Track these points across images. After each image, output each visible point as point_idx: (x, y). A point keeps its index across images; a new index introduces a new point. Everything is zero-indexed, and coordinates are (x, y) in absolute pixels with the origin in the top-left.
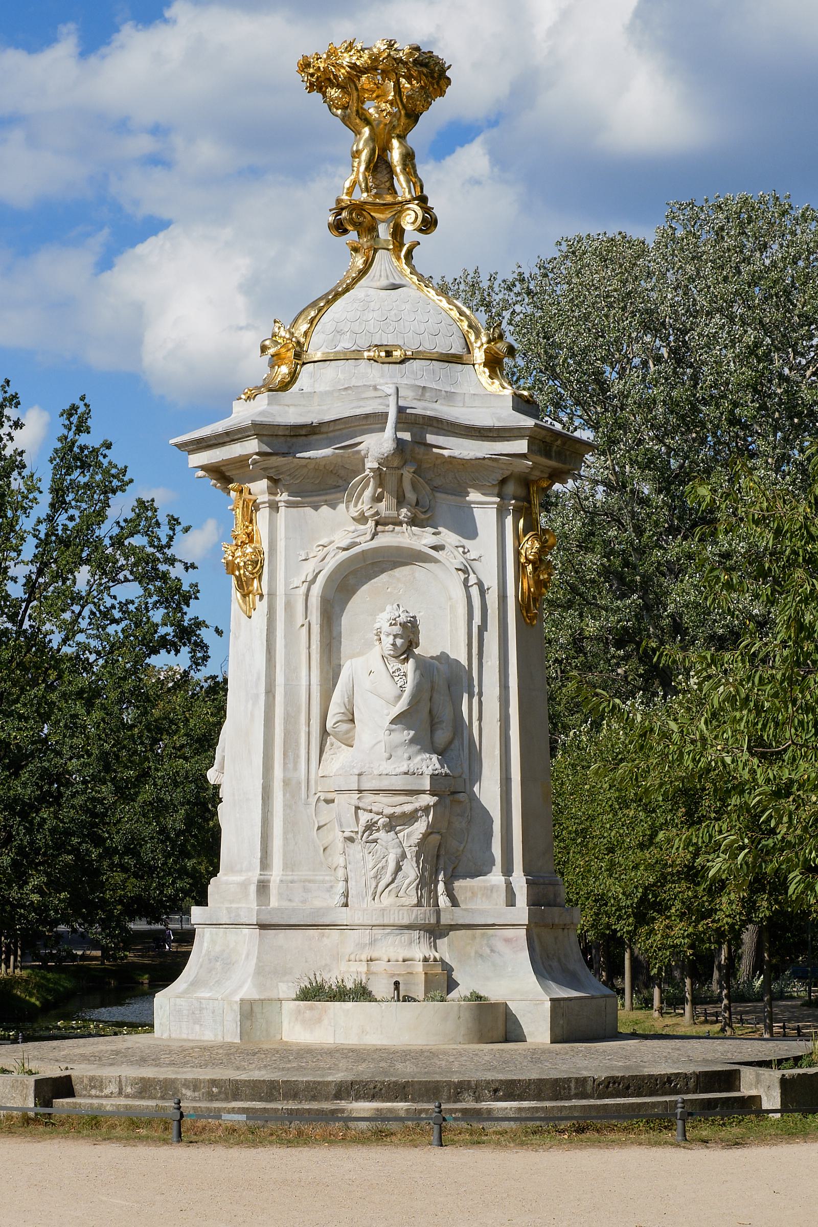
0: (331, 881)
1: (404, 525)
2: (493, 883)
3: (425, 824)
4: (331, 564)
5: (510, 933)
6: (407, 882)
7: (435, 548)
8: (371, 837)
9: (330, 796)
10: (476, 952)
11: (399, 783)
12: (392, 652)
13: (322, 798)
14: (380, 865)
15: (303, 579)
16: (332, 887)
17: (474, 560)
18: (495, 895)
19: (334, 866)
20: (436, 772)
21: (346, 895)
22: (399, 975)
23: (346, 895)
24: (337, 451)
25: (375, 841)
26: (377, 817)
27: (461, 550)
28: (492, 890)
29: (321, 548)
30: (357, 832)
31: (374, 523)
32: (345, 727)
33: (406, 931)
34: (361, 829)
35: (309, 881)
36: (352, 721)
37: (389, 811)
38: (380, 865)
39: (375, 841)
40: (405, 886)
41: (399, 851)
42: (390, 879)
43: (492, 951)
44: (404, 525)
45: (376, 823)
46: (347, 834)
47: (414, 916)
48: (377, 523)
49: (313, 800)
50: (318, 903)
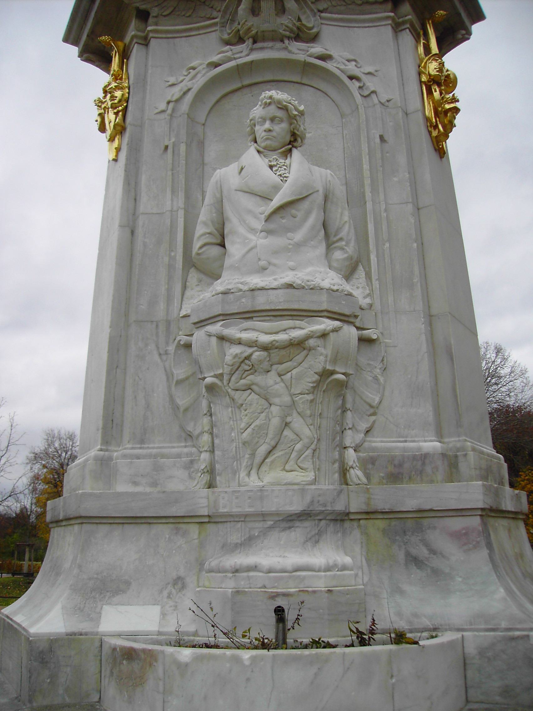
0: (191, 454)
1: (286, 41)
2: (425, 451)
3: (322, 358)
4: (200, 81)
5: (457, 524)
6: (298, 446)
8: (243, 382)
10: (408, 554)
11: (279, 300)
12: (268, 142)
13: (182, 343)
14: (257, 422)
15: (169, 98)
16: (192, 462)
17: (369, 73)
18: (428, 469)
19: (196, 433)
20: (335, 288)
21: (211, 471)
22: (285, 595)
23: (211, 471)
25: (249, 388)
26: (249, 351)
28: (424, 464)
29: (191, 71)
30: (220, 376)
31: (251, 40)
32: (216, 251)
33: (298, 524)
34: (227, 370)
35: (163, 456)
36: (223, 245)
37: (265, 339)
38: (257, 422)
39: (249, 388)
40: (294, 455)
41: (287, 399)
42: (273, 443)
43: (433, 552)
44: (286, 41)
45: (248, 358)
46: (209, 380)
47: (308, 499)
48: (255, 42)
49: (171, 348)
50: (174, 486)
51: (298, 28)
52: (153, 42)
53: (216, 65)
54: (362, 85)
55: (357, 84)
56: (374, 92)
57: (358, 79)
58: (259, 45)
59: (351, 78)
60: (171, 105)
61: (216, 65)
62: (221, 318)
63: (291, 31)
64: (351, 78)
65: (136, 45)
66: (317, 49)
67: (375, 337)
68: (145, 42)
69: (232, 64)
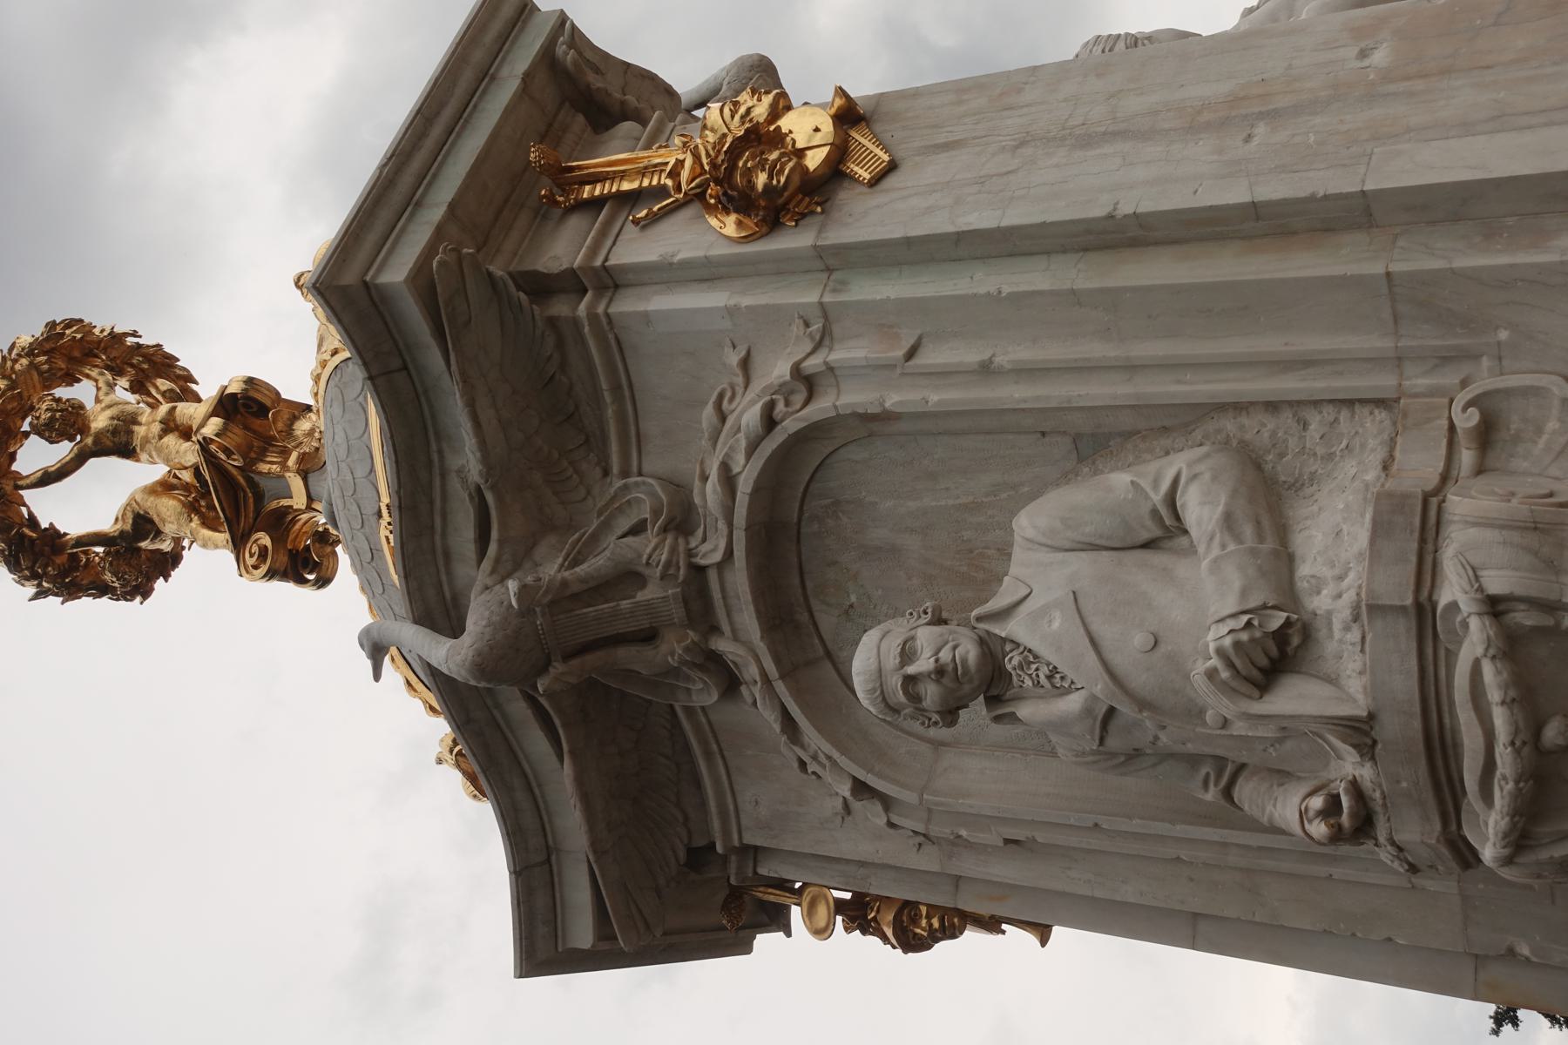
48: (715, 629)
52: (749, 839)
56: (796, 370)
57: (770, 407)
59: (770, 422)
60: (895, 819)
63: (673, 550)
66: (710, 494)
68: (754, 853)
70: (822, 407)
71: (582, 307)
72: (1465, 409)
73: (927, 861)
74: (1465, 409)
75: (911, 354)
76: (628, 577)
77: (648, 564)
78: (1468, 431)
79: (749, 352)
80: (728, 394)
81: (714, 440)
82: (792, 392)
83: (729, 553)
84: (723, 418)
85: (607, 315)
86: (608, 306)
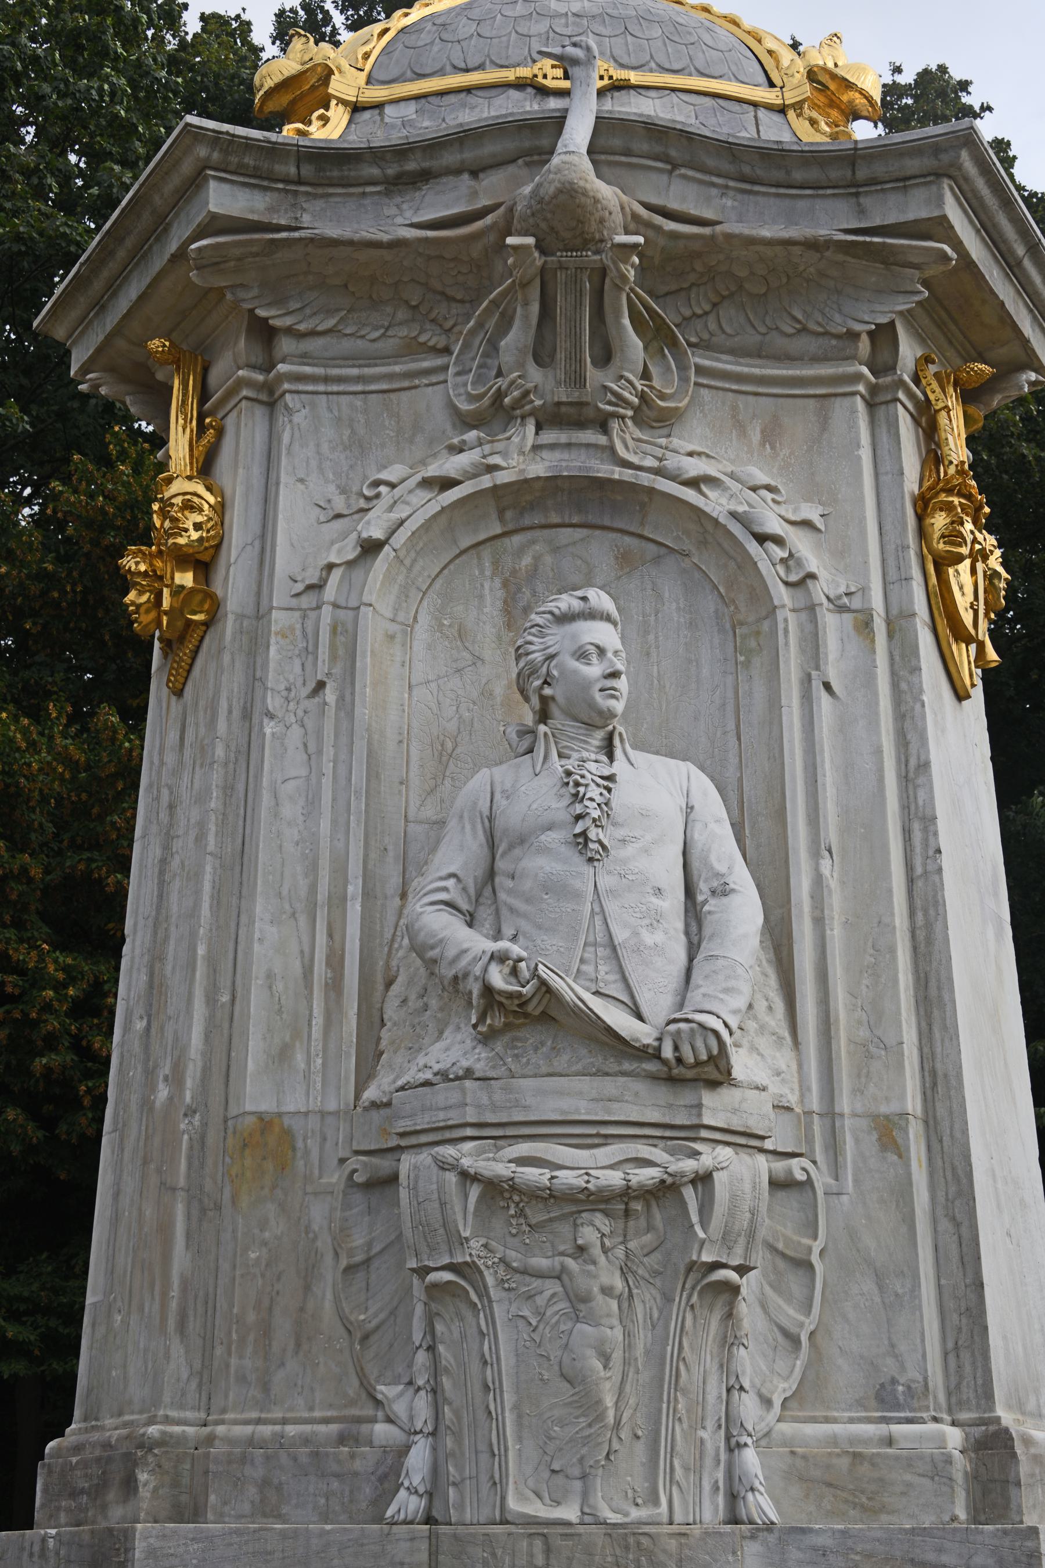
7: (694, 483)
9: (384, 1165)
24: (430, 234)
27: (769, 496)
48: (539, 428)
51: (642, 396)
53: (447, 484)
54: (786, 555)
55: (779, 553)
56: (812, 576)
57: (779, 541)
58: (549, 436)
59: (762, 539)
60: (336, 575)
61: (447, 484)
62: (469, 1132)
64: (762, 539)
65: (244, 402)
67: (801, 1176)
68: (270, 399)
69: (486, 482)
70: (782, 595)
71: (865, 370)
72: (804, 1169)
73: (280, 594)
74: (804, 1169)
75: (827, 686)
76: (605, 357)
77: (622, 377)
78: (790, 1172)
79: (819, 530)
80: (779, 499)
81: (732, 476)
82: (788, 569)
83: (626, 464)
84: (754, 489)
85: (854, 394)
86: (862, 397)
